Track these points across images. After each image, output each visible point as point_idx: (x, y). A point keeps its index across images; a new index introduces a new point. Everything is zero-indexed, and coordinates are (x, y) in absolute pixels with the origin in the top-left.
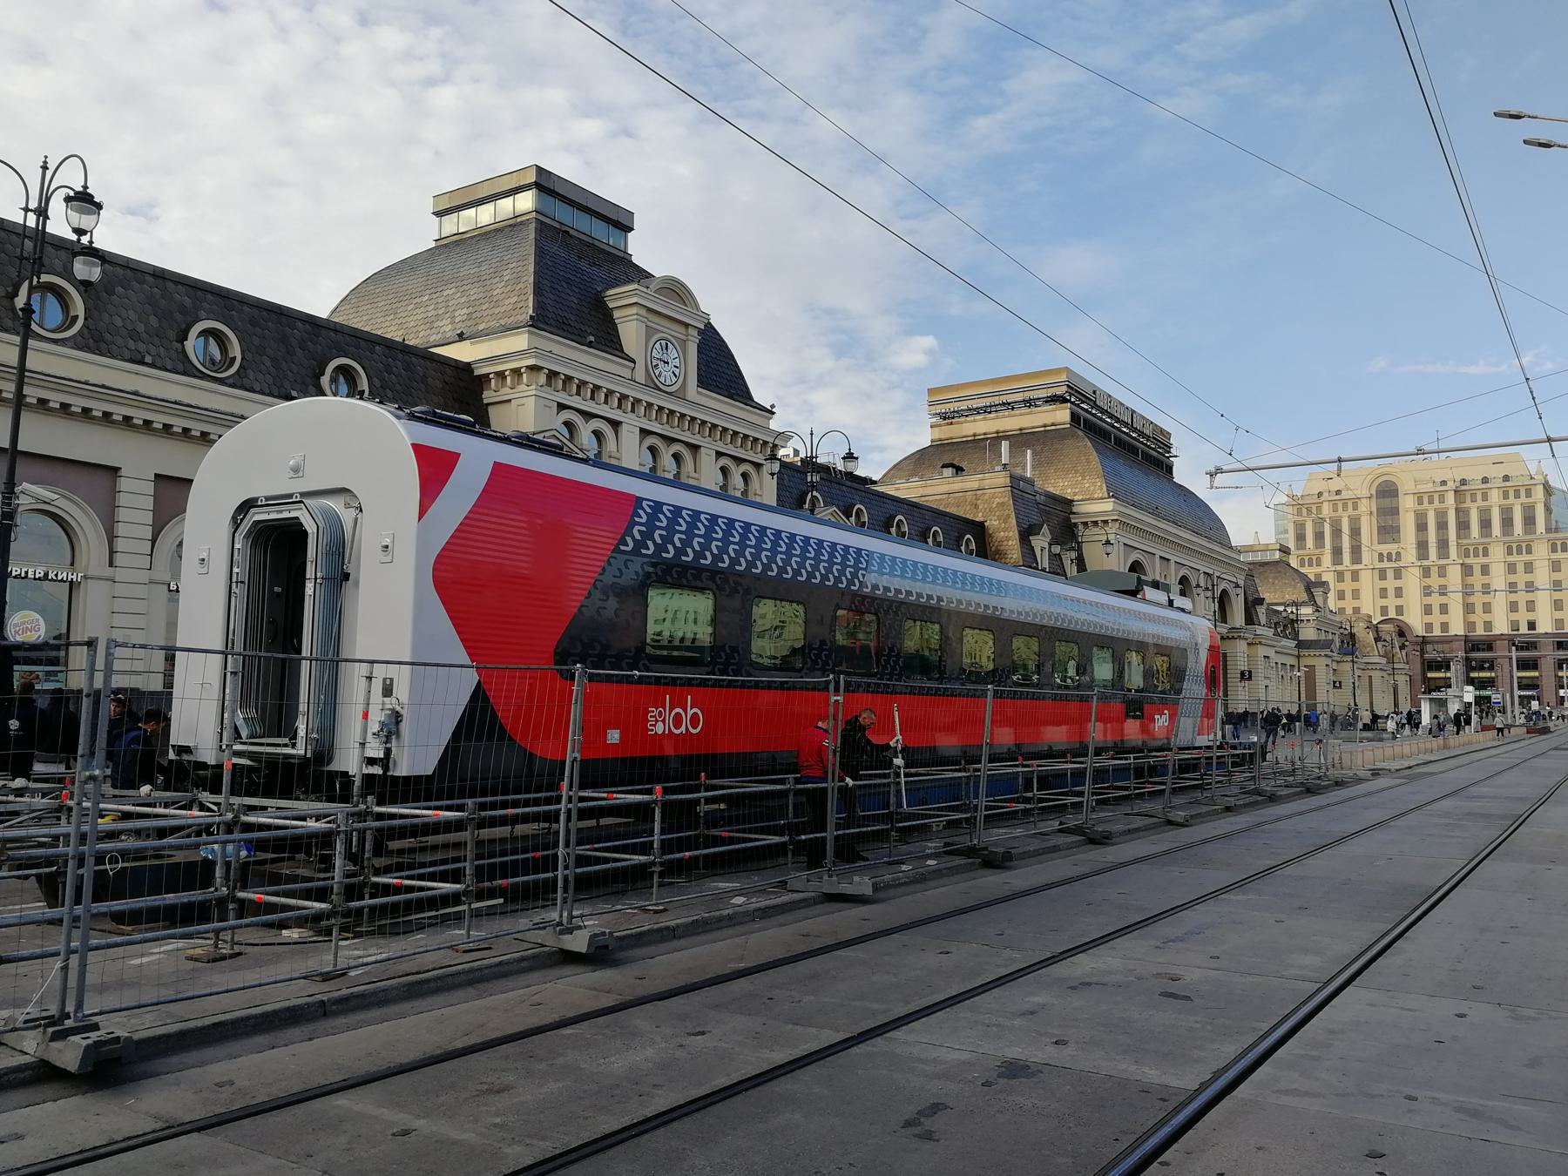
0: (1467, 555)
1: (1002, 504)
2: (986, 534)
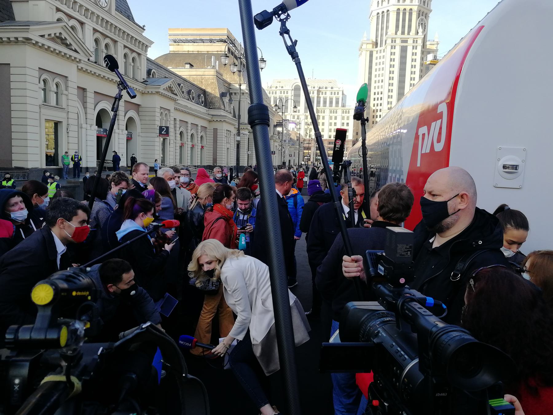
1: (212, 83)
2: (206, 94)
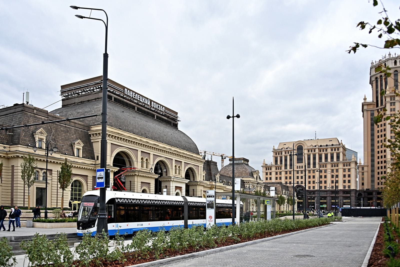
0: (321, 167)
